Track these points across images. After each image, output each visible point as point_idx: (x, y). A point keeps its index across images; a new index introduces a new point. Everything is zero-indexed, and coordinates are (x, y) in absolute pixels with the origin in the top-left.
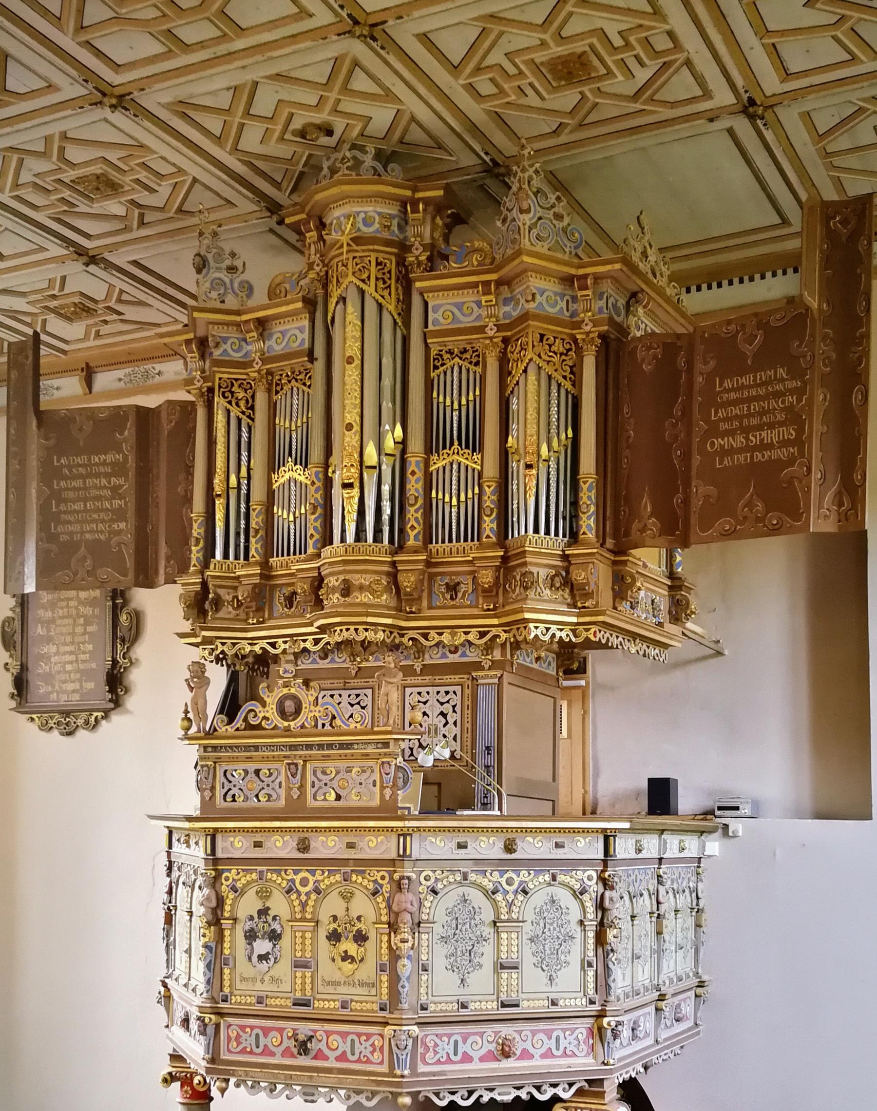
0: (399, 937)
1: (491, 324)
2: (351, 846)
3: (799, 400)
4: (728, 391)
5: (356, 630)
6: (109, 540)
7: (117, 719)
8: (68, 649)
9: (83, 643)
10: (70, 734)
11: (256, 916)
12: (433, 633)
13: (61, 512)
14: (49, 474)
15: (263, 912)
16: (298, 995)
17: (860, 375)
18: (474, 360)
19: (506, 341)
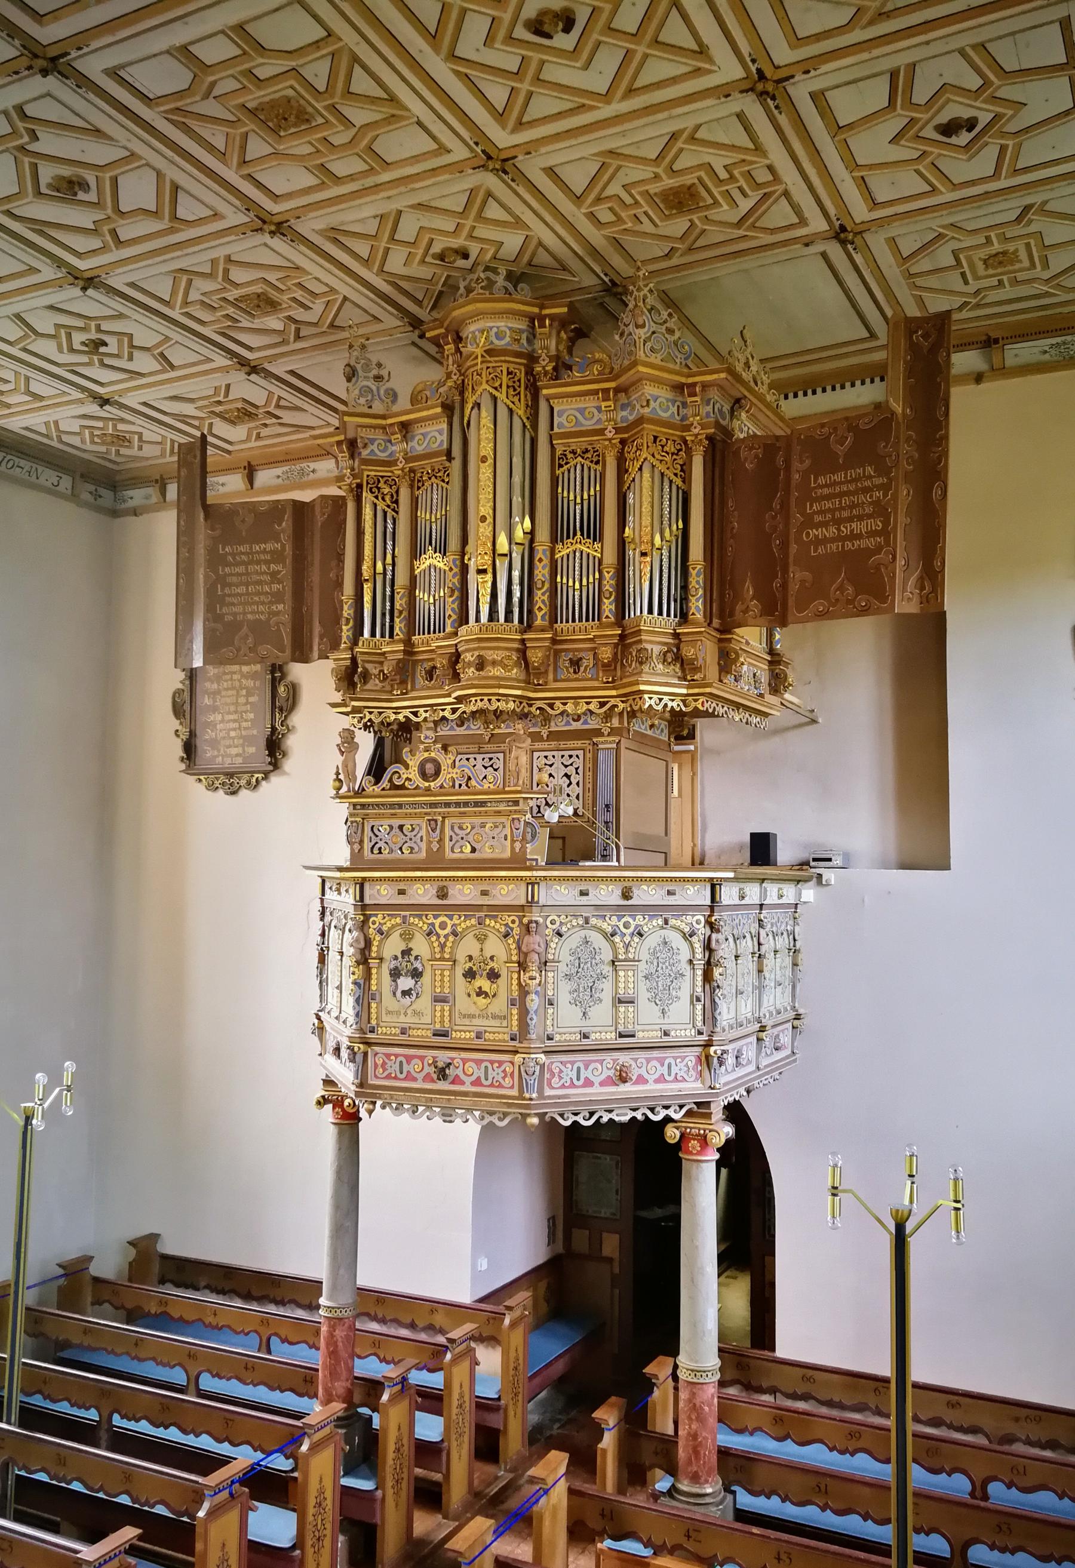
0: (527, 975)
1: (610, 427)
2: (484, 893)
3: (885, 495)
4: (822, 487)
5: (489, 700)
6: (269, 619)
7: (274, 779)
8: (232, 717)
9: (245, 712)
10: (234, 793)
11: (400, 956)
12: (558, 703)
13: (225, 595)
14: (215, 561)
15: (406, 952)
16: (438, 1026)
17: (939, 473)
18: (595, 460)
19: (623, 442)
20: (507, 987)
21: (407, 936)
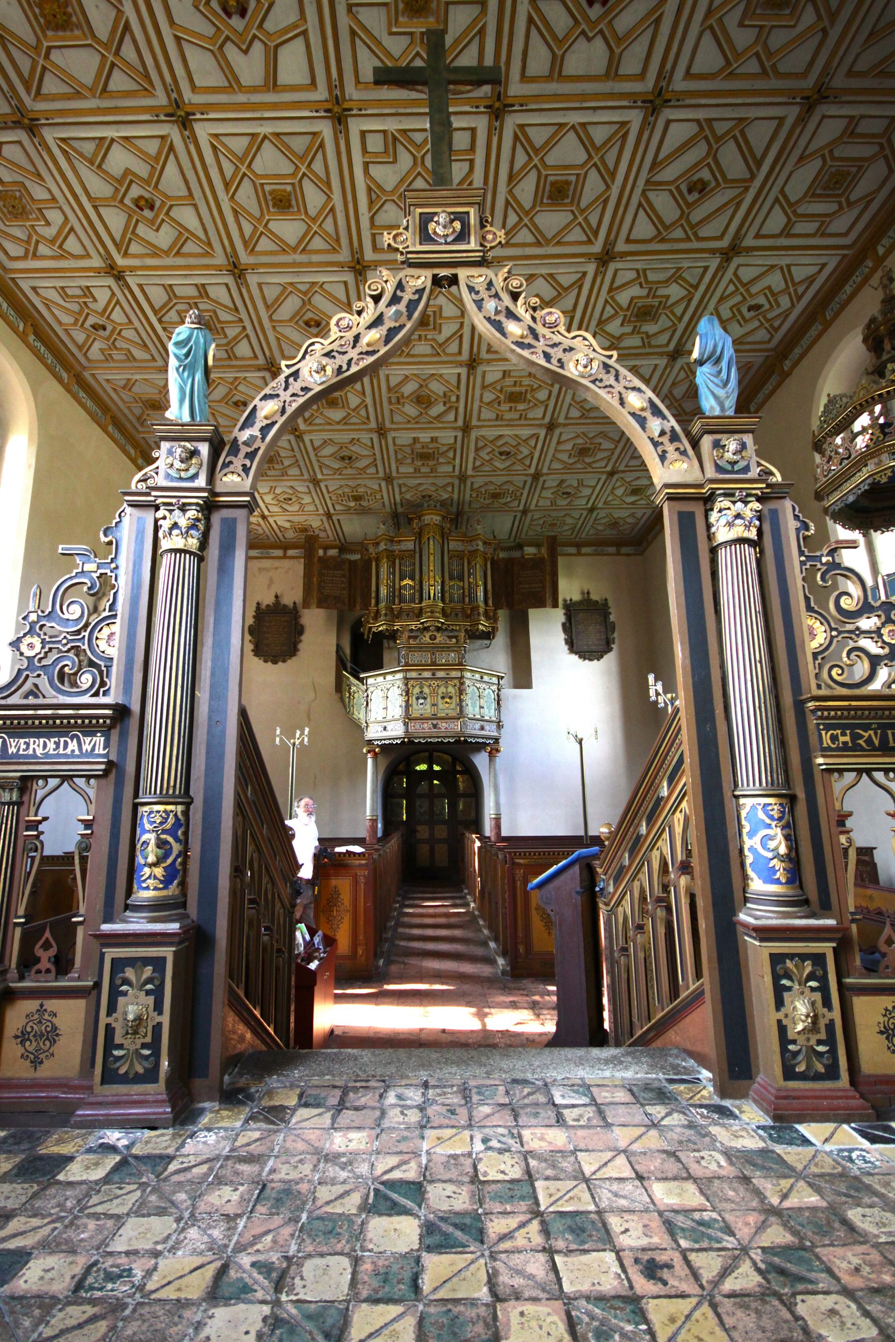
20: (455, 700)
21: (421, 687)
